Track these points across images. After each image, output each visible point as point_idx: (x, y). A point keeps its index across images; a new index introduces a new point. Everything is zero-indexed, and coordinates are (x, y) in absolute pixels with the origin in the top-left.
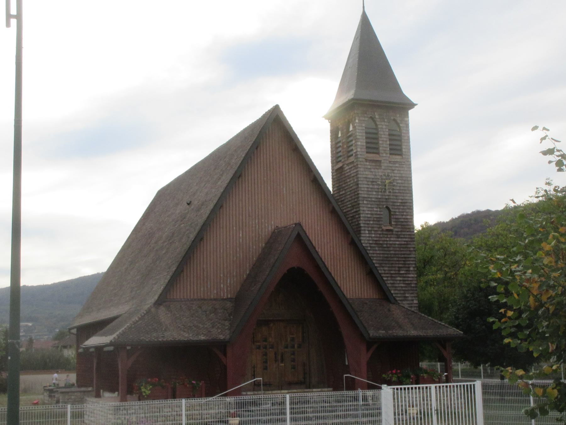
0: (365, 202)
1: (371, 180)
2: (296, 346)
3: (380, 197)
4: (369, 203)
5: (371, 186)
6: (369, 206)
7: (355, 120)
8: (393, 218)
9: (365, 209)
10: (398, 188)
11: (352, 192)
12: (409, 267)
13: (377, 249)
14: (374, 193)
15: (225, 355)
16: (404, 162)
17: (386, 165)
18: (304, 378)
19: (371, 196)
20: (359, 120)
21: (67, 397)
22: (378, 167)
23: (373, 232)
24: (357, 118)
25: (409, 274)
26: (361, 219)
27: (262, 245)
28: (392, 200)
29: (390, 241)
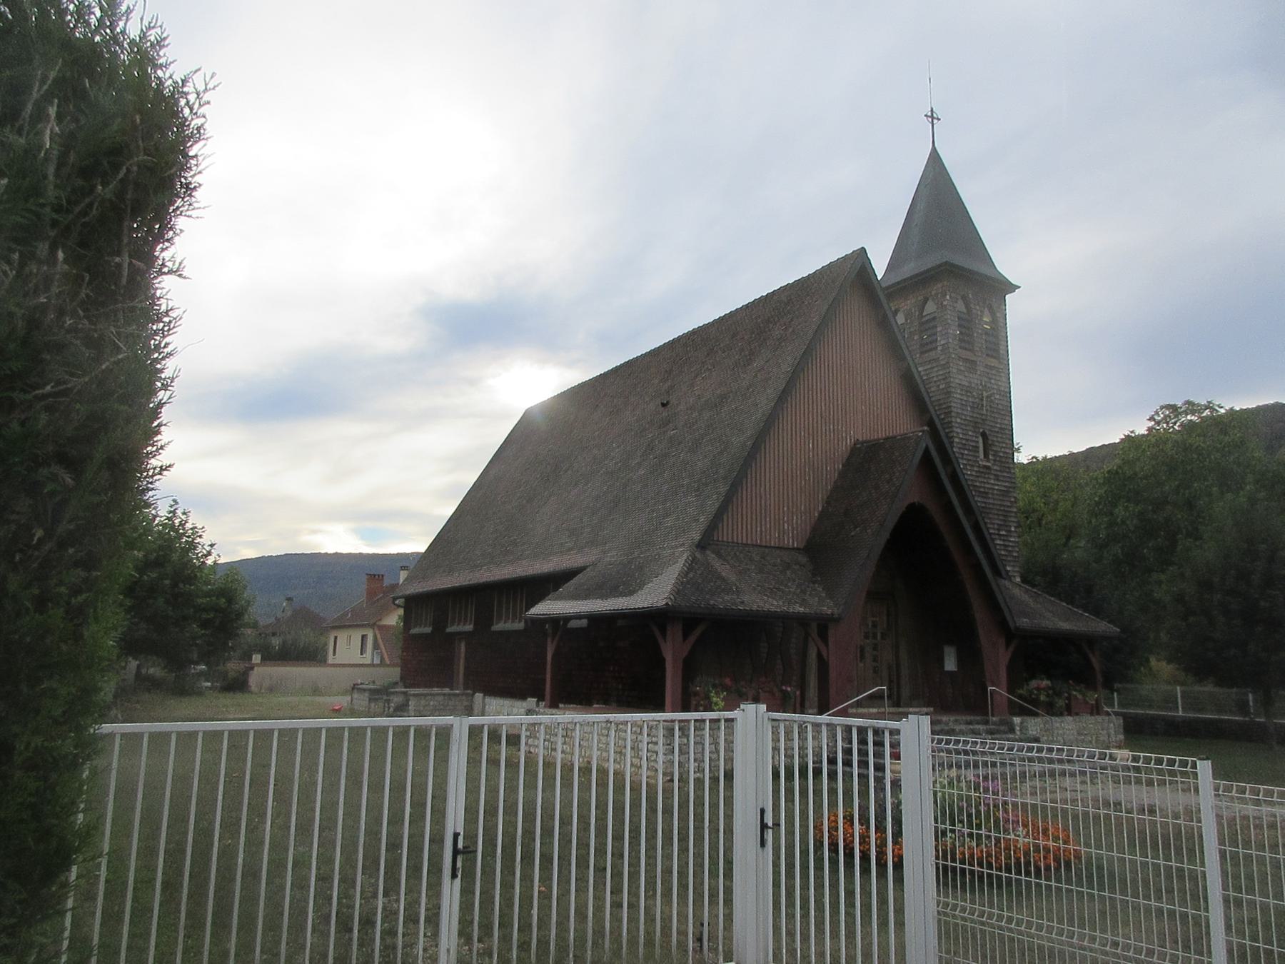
0: (959, 420)
3: (975, 415)
9: (959, 431)
12: (1010, 526)
20: (950, 297)
21: (423, 702)
23: (968, 467)
24: (948, 293)
25: (1011, 536)
27: (838, 467)
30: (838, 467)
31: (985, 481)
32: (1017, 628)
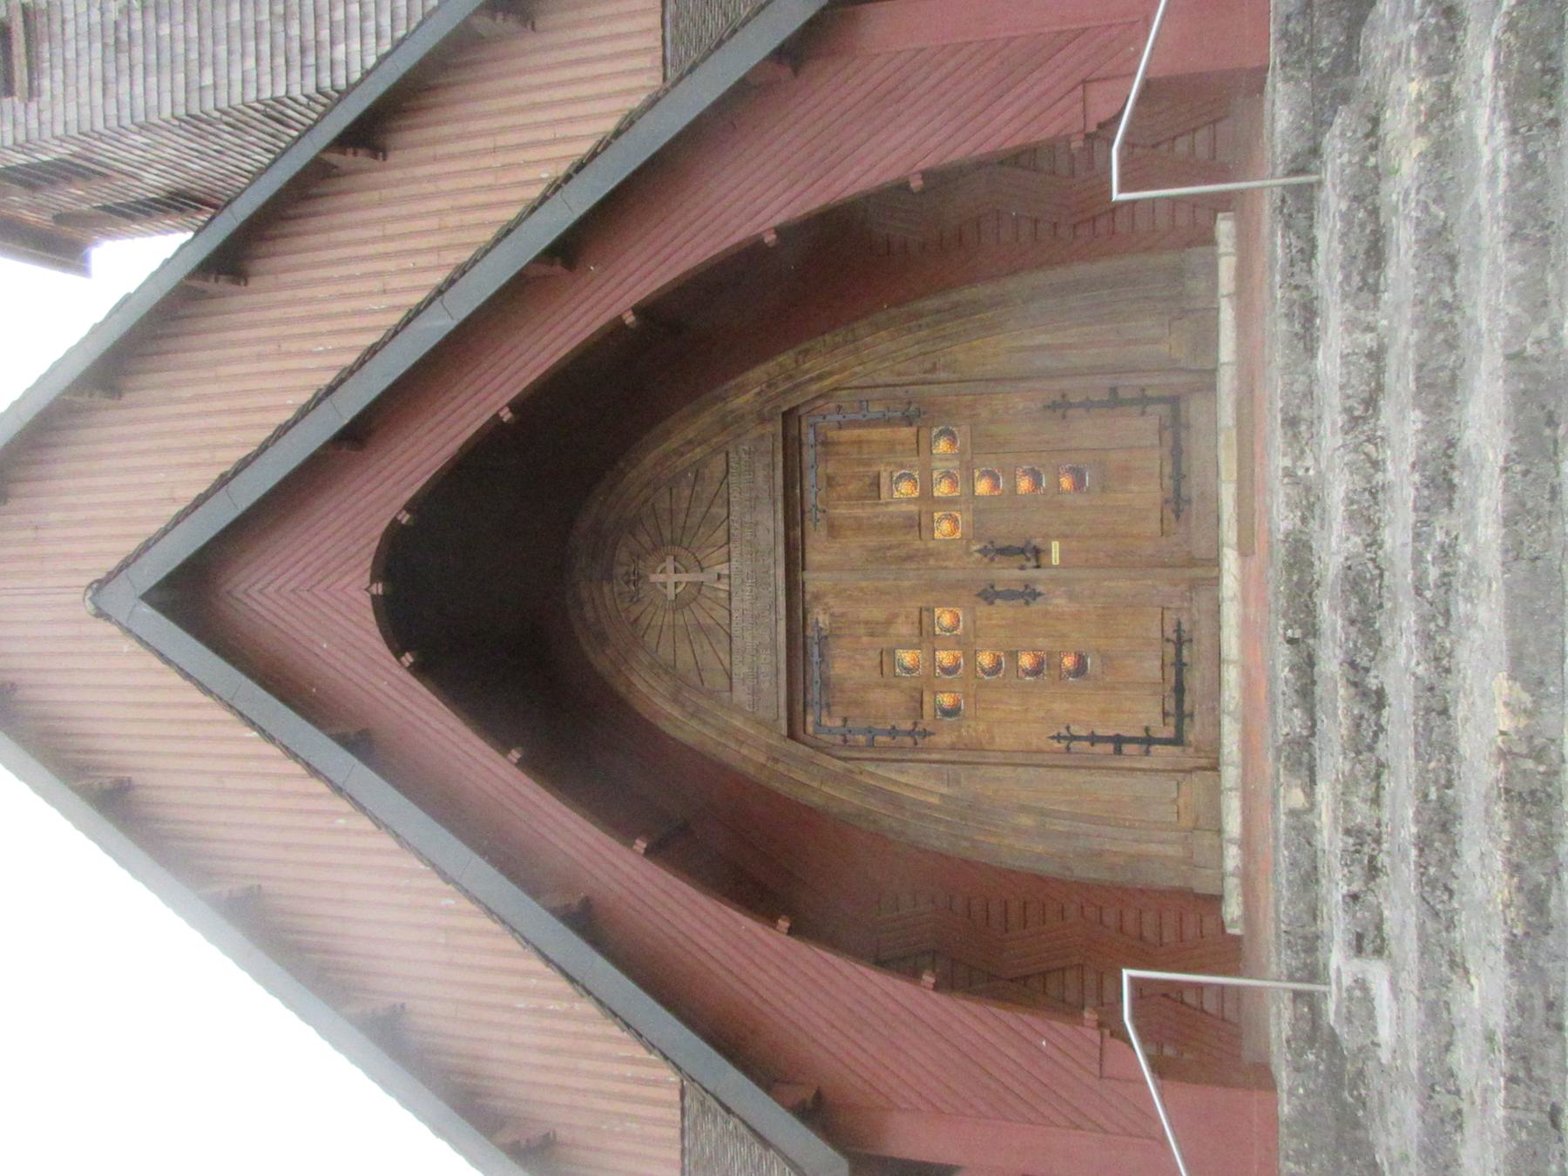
0: (208, 80)
4: (208, 59)
6: (222, 50)
9: (236, 76)
14: (165, 30)
18: (1143, 401)
22: (57, 28)
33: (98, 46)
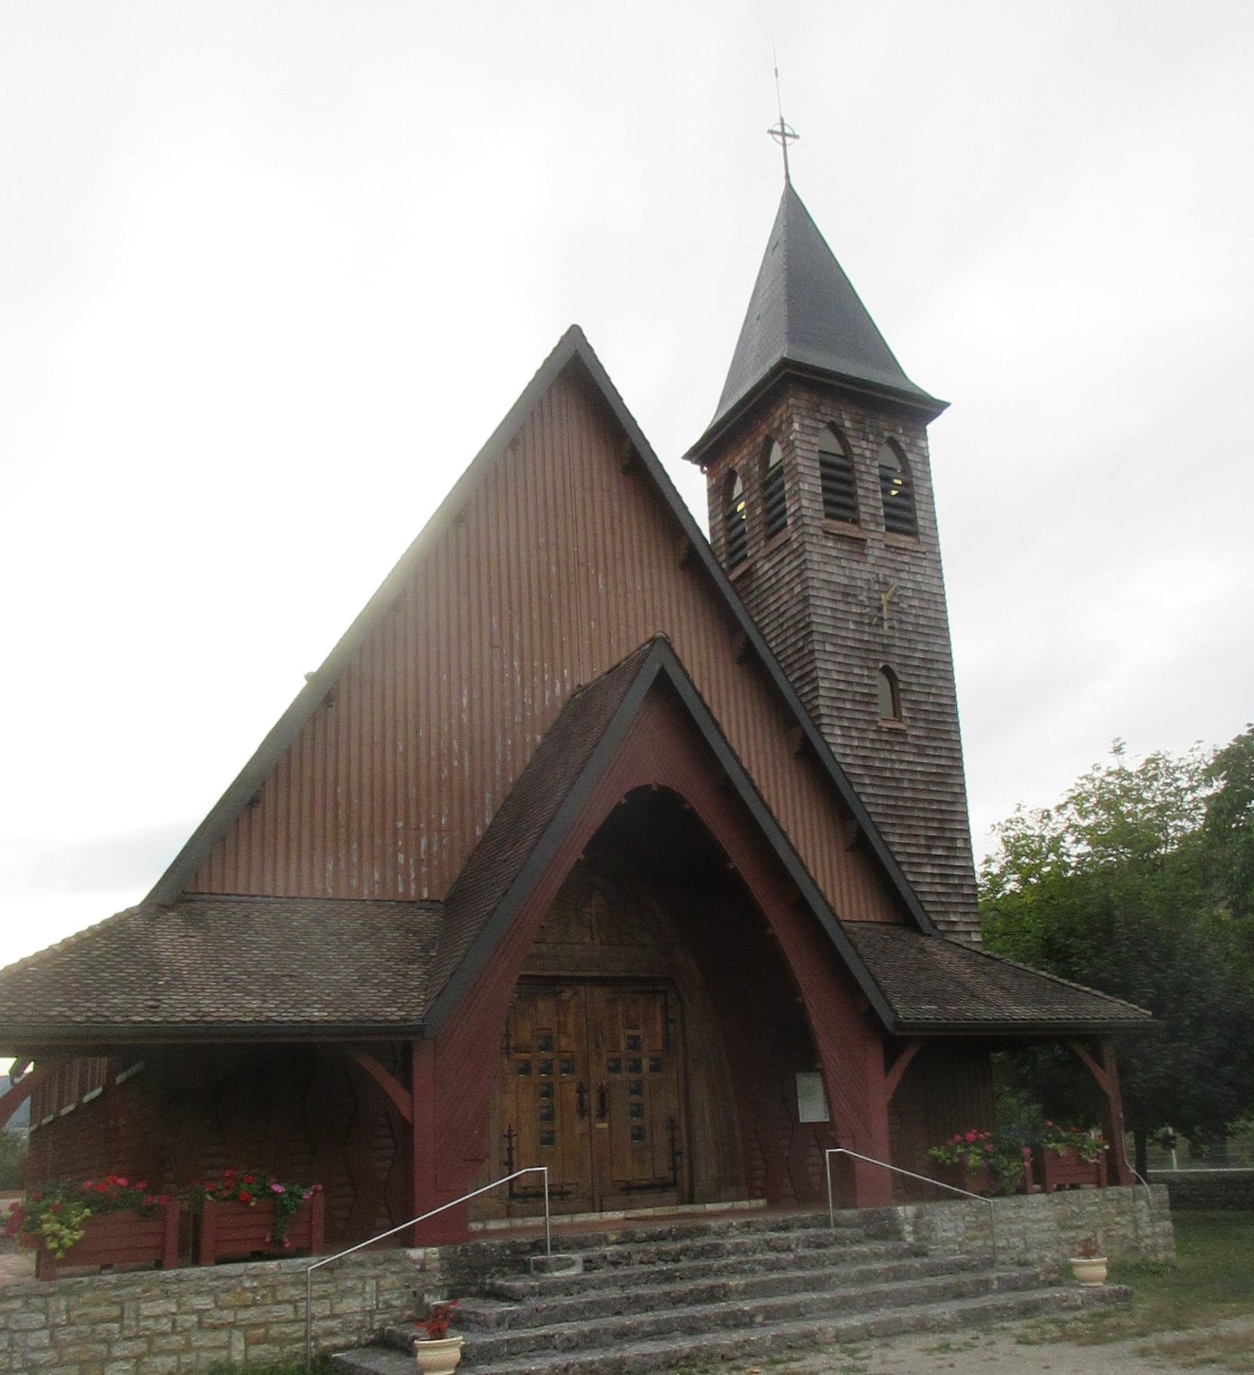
0: (829, 648)
1: (841, 589)
2: (646, 1064)
5: (841, 607)
6: (840, 659)
7: (791, 423)
8: (906, 700)
9: (829, 666)
10: (911, 619)
11: (785, 626)
13: (867, 781)
14: (852, 626)
15: (408, 1085)
16: (924, 553)
17: (877, 553)
19: (843, 633)
26: (822, 692)
28: (898, 651)
29: (901, 761)
30: (534, 740)
31: (893, 757)
32: (899, 1025)
33: (845, 581)
